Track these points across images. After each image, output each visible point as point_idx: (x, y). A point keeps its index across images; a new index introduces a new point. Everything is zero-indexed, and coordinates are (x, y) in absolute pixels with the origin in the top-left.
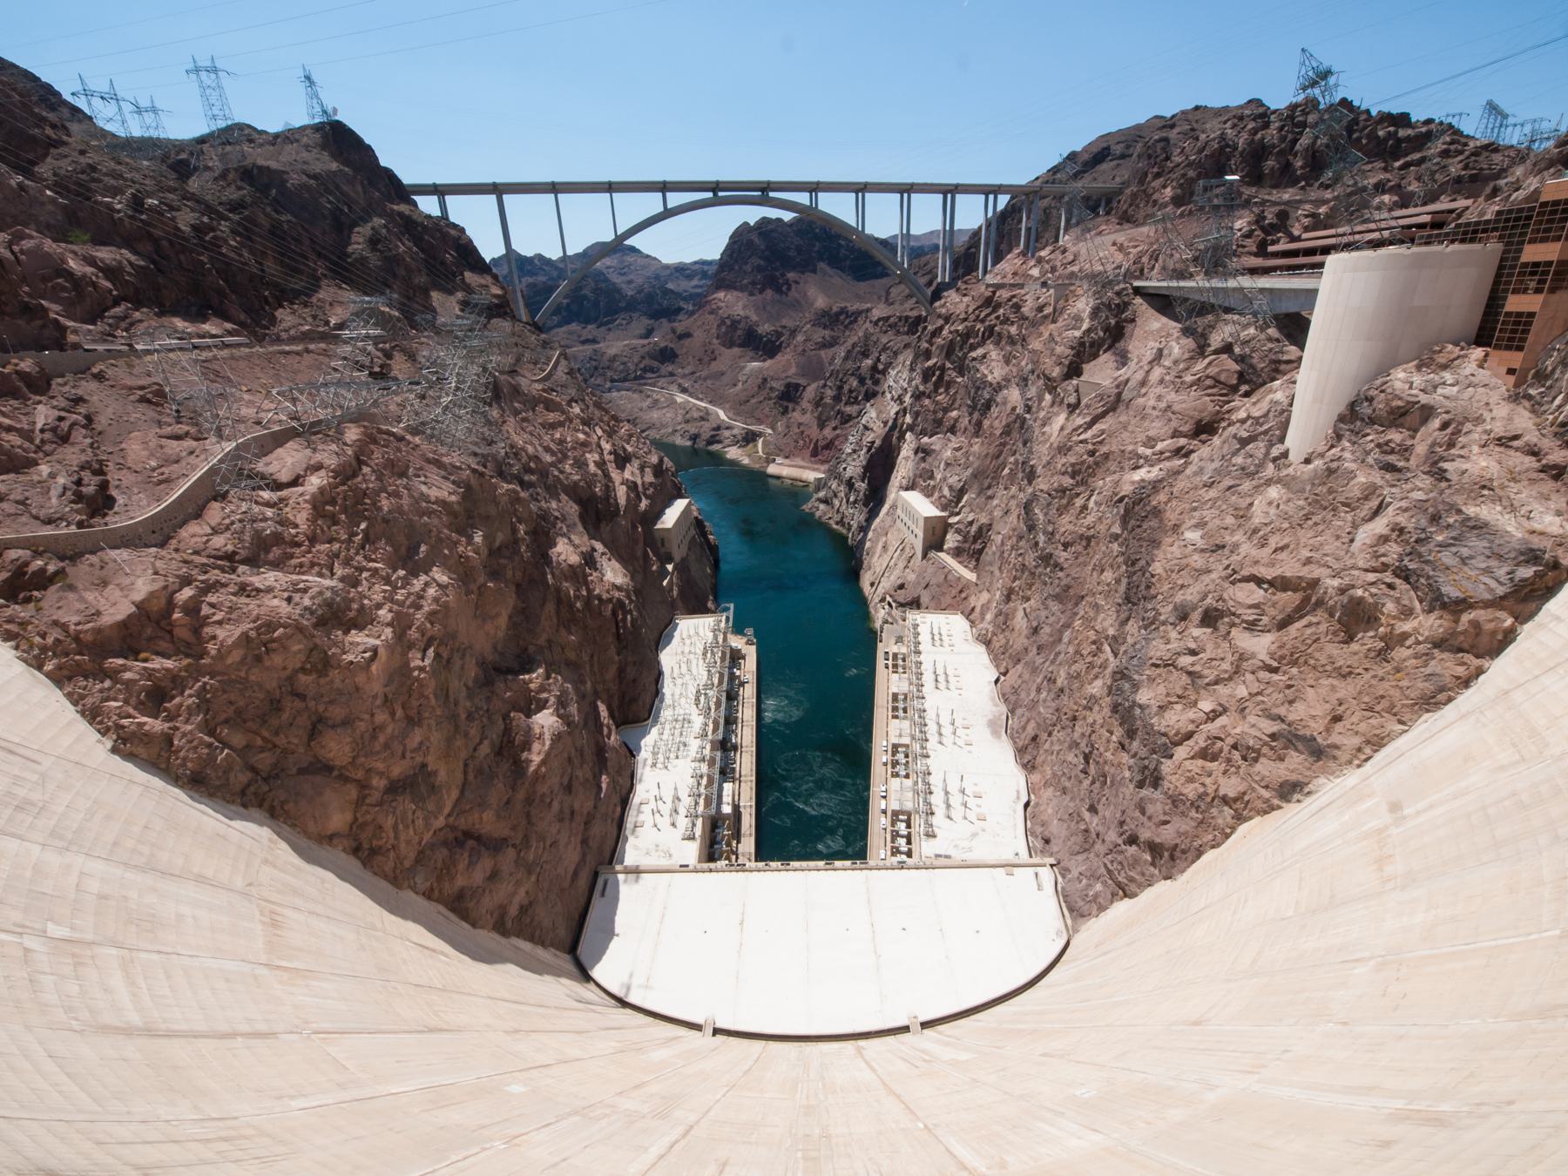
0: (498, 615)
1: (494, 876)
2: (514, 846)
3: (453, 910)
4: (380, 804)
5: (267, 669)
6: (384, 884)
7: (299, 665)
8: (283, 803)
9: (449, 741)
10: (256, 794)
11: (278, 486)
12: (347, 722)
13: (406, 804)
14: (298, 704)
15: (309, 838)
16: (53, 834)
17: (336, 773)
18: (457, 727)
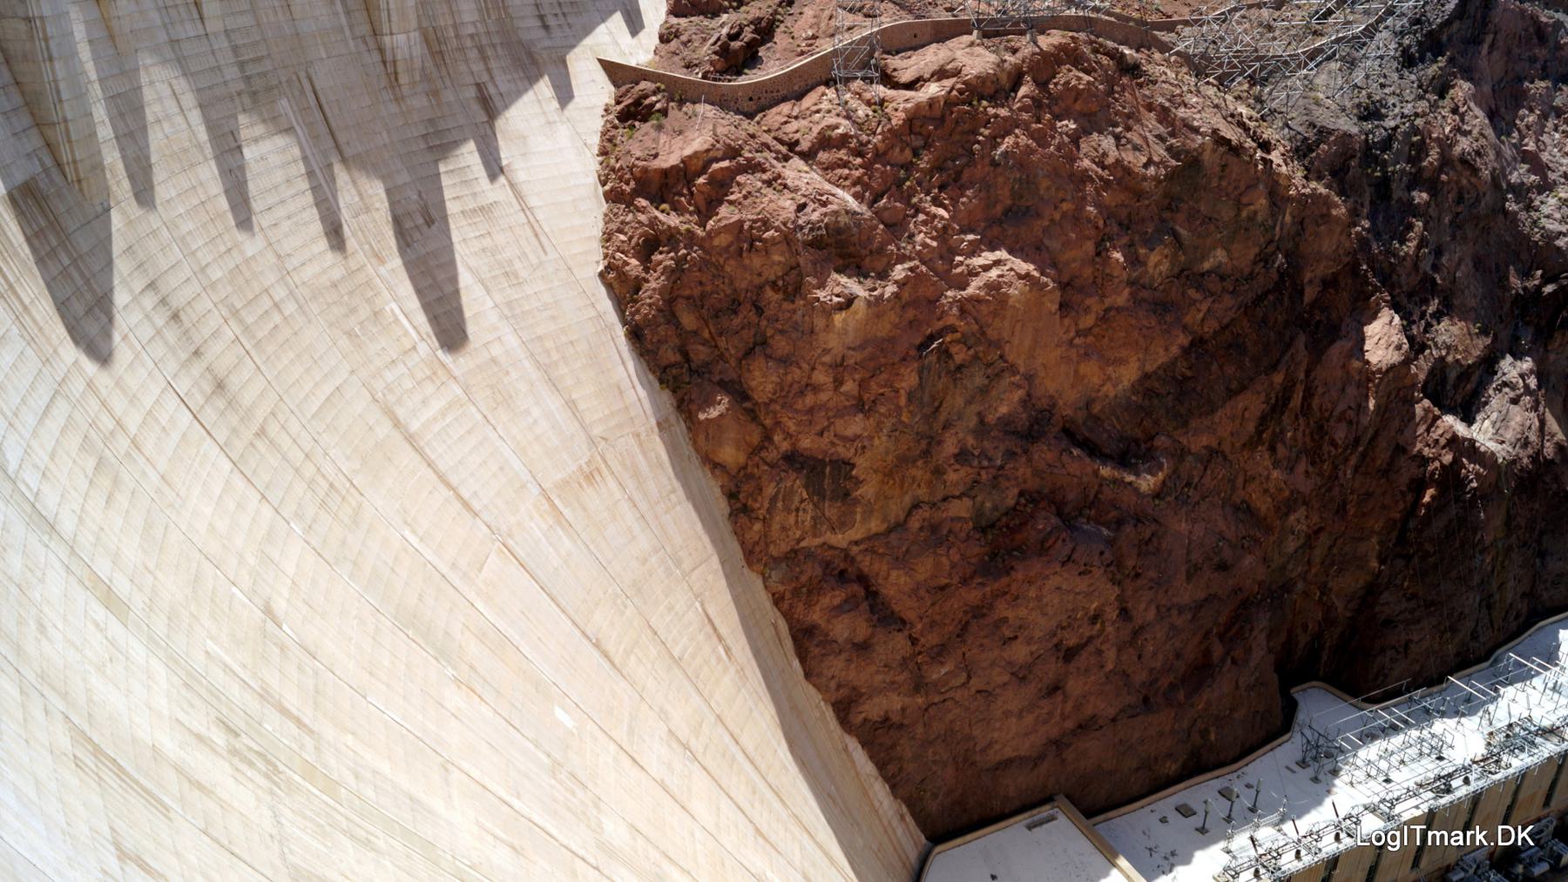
0: (1121, 362)
1: (863, 648)
2: (914, 641)
3: (795, 639)
4: (772, 466)
5: (745, 268)
6: (735, 547)
7: (772, 278)
8: (691, 401)
9: (904, 461)
10: (675, 378)
11: (896, 86)
12: (785, 361)
13: (796, 484)
14: (752, 316)
15: (697, 451)
16: (509, 304)
17: (747, 405)
18: (926, 453)
